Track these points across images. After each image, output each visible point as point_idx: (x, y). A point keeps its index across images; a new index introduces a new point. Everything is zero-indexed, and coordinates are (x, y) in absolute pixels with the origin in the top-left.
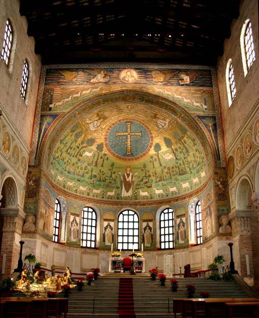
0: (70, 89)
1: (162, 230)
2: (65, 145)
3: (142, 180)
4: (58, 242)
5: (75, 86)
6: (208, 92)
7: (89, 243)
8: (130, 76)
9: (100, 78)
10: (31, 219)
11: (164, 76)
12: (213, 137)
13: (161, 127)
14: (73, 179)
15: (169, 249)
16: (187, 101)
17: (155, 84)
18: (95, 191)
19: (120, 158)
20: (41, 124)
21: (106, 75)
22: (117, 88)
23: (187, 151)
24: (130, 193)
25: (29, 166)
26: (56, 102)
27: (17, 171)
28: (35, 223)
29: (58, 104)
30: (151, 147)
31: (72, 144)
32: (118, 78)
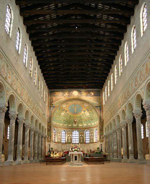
1: (86, 137)
3: (80, 121)
4: (55, 142)
7: (63, 141)
8: (75, 93)
9: (66, 94)
10: (49, 137)
14: (58, 122)
15: (88, 143)
18: (65, 125)
19: (73, 114)
20: (50, 109)
22: (71, 97)
23: (93, 114)
24: (76, 125)
25: (48, 122)
27: (45, 124)
28: (51, 139)
30: (82, 111)
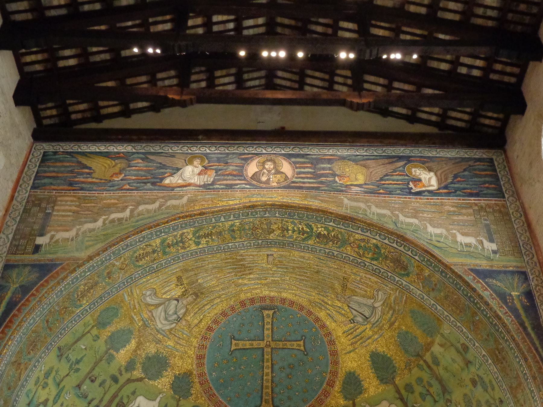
0: (102, 199)
2: (74, 366)
5: (120, 193)
6: (494, 211)
11: (364, 170)
12: (529, 329)
13: (359, 319)
16: (438, 231)
17: (342, 191)
21: (206, 168)
23: (445, 390)
26: (57, 231)
29: (62, 235)
30: (331, 384)
31: (96, 364)
32: (240, 175)
